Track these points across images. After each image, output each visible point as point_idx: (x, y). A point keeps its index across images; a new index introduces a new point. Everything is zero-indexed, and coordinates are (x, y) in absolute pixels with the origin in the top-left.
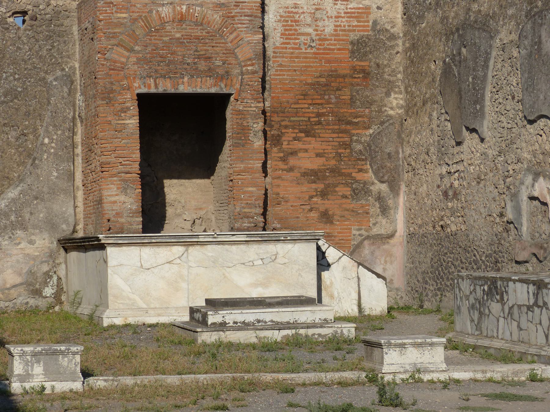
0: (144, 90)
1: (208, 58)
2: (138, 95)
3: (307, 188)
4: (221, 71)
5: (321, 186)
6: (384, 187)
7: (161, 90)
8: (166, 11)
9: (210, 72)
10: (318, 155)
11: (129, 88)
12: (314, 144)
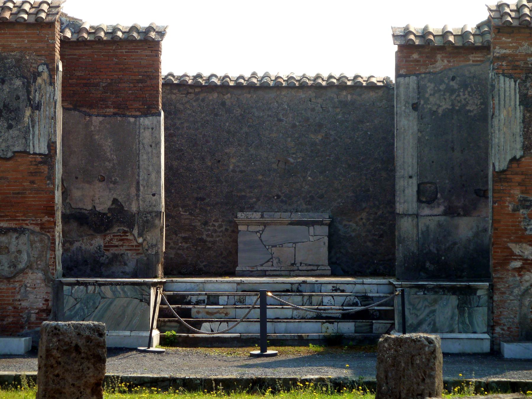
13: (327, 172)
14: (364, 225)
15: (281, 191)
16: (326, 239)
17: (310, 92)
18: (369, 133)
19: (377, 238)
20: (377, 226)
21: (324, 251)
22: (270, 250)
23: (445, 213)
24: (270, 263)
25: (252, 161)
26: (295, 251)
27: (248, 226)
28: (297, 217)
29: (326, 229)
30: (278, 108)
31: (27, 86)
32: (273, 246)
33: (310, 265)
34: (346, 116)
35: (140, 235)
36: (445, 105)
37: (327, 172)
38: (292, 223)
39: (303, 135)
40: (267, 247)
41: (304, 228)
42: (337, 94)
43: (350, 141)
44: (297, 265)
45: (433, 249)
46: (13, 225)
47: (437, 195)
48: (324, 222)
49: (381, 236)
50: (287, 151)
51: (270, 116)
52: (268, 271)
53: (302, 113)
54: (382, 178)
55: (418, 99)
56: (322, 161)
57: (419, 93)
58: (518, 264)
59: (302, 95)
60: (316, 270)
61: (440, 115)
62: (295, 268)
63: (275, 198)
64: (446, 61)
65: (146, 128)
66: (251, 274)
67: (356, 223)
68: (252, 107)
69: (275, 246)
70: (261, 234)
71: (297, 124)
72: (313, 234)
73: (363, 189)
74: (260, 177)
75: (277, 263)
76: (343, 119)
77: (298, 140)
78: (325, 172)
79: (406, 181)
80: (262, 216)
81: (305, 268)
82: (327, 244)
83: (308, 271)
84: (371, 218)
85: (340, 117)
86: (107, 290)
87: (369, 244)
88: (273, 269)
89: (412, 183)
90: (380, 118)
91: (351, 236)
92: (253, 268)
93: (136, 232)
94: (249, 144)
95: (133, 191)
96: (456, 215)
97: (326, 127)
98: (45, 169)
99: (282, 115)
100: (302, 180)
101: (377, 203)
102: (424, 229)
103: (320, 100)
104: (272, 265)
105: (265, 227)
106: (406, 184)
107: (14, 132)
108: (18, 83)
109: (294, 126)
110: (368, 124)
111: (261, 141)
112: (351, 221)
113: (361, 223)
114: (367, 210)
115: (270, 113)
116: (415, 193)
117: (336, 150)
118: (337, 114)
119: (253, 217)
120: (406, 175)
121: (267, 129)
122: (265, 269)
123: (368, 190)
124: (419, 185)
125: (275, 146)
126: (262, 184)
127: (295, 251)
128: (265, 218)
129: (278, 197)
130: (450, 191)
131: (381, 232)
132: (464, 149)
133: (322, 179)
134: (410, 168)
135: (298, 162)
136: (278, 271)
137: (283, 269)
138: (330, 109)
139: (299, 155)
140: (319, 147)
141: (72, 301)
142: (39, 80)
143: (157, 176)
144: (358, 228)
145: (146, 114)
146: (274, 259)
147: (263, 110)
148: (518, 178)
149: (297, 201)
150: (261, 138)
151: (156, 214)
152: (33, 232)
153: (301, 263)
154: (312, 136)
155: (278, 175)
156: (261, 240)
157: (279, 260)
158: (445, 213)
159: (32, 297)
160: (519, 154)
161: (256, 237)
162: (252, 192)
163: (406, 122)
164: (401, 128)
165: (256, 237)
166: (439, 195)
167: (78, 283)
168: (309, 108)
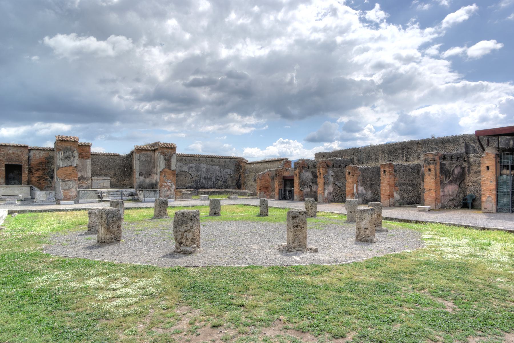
0: (6, 164)
1: (18, 159)
2: (6, 165)
3: (37, 179)
4: (20, 161)
5: (39, 179)
6: (51, 179)
7: (9, 164)
8: (11, 152)
9: (19, 161)
10: (39, 174)
11: (3, 163)
12: (38, 173)
23: (144, 178)
28: (104, 178)
31: (72, 153)
35: (87, 181)
36: (144, 159)
41: (105, 180)
45: (142, 184)
46: (69, 179)
58: (164, 186)
59: (104, 156)
65: (88, 162)
86: (89, 192)
93: (86, 181)
95: (85, 173)
98: (76, 169)
107: (69, 162)
108: (70, 152)
141: (81, 194)
142: (75, 152)
145: (88, 159)
148: (164, 172)
152: (73, 181)
158: (144, 178)
159: (73, 193)
160: (164, 168)
161: (96, 182)
165: (96, 182)
167: (83, 191)
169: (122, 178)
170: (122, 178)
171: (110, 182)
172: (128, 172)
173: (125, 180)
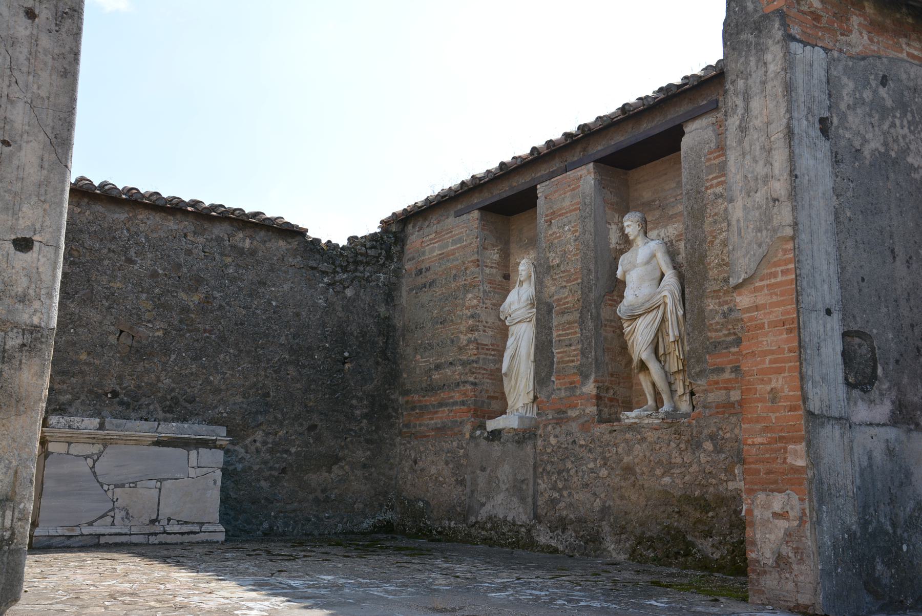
13: (204, 359)
14: (258, 451)
15: (120, 384)
16: (218, 474)
17: (187, 223)
18: (274, 303)
19: (276, 473)
20: (278, 455)
21: (214, 497)
22: (110, 493)
23: (894, 421)
24: (108, 520)
25: (71, 326)
26: (159, 496)
27: (69, 443)
28: (170, 429)
29: (219, 455)
30: (129, 240)
32: (116, 486)
33: (186, 523)
34: (240, 272)
37: (204, 359)
38: (158, 443)
39: (168, 291)
40: (106, 487)
41: (180, 452)
42: (228, 235)
43: (244, 312)
44: (161, 524)
47: (875, 369)
48: (217, 443)
49: (284, 471)
50: (138, 315)
51: (114, 252)
52: (104, 535)
53: (169, 256)
54: (289, 377)
55: (830, 108)
56: (198, 340)
57: (830, 95)
59: (172, 224)
60: (198, 533)
61: (867, 162)
62: (158, 528)
63: (109, 395)
64: (866, 37)
66: (68, 543)
67: (246, 447)
68: (81, 231)
69: (123, 486)
70: (95, 462)
71: (160, 272)
72: (195, 465)
73: (260, 392)
74: (84, 357)
75: (122, 518)
76: (236, 274)
77: (159, 299)
78: (201, 358)
79: (821, 322)
80: (102, 427)
81: (176, 528)
82: (219, 483)
83: (182, 534)
84: (270, 440)
85: (231, 271)
87: (263, 484)
88: (113, 531)
89: (832, 329)
90: (292, 283)
91: (235, 469)
92: (73, 530)
94: (68, 294)
96: (912, 427)
97: (207, 285)
99: (135, 253)
100: (160, 369)
101: (279, 416)
102: (865, 463)
103: (201, 240)
104: (113, 524)
105: (105, 447)
106: (822, 330)
109: (154, 275)
110: (273, 289)
111: (92, 293)
112: (238, 443)
113: (253, 448)
114: (264, 427)
115: (113, 247)
116: (839, 359)
117: (221, 323)
118: (227, 266)
119: (83, 426)
120: (820, 306)
121: (105, 273)
122: (98, 532)
123: (268, 395)
124: (845, 335)
125: (117, 305)
126: (86, 368)
127: (159, 496)
128: (108, 430)
129: (115, 394)
130: (897, 362)
131: (284, 465)
132: (911, 258)
133: (194, 370)
134: (826, 287)
135: (154, 337)
136: (126, 534)
137: (134, 530)
138: (217, 257)
139: (158, 324)
140: (193, 316)
143: (50, 157)
144: (249, 456)
146: (117, 511)
147: (101, 240)
149: (148, 405)
150: (93, 286)
151: (28, 338)
153: (169, 520)
154: (183, 295)
155: (118, 355)
156: (94, 473)
157: (127, 513)
158: (894, 421)
161: (84, 467)
162: (64, 382)
163: (811, 162)
164: (803, 175)
166: (880, 371)
168: (182, 249)
169: (318, 439)
170: (318, 439)
171: (228, 473)
172: (369, 387)
173: (336, 460)
